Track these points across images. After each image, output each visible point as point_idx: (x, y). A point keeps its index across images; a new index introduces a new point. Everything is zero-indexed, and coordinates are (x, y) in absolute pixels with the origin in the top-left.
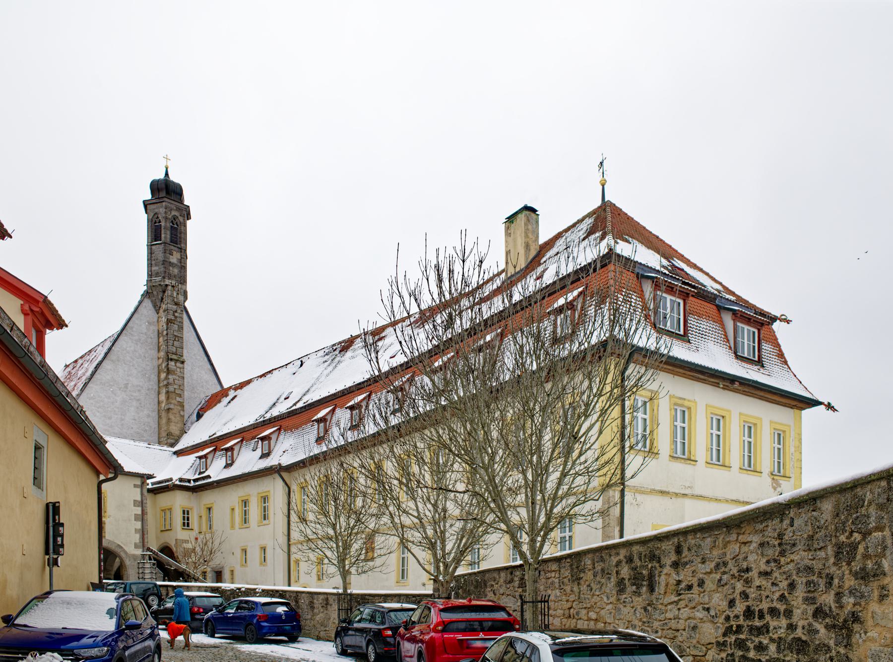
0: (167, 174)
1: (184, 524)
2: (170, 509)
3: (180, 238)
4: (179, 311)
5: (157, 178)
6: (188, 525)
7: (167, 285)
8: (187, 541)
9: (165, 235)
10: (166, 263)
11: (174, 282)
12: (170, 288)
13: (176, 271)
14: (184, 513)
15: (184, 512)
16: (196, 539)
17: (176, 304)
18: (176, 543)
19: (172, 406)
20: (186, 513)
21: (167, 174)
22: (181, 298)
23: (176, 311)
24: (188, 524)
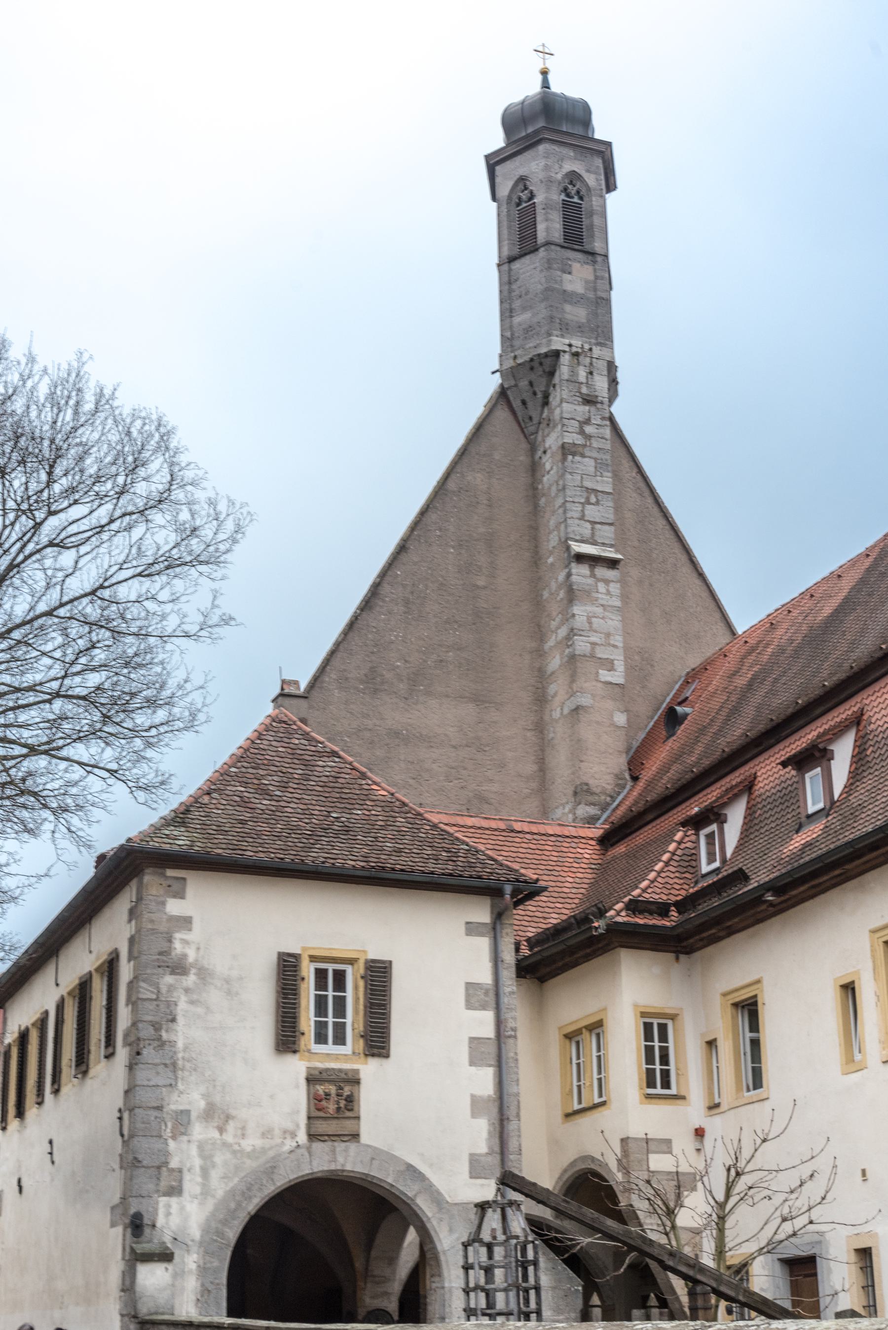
0: (546, 85)
1: (650, 1074)
2: (599, 1024)
3: (591, 227)
4: (596, 420)
5: (517, 98)
6: (666, 1084)
7: (557, 354)
8: (665, 1146)
9: (549, 226)
10: (554, 295)
11: (577, 343)
12: (565, 359)
13: (577, 313)
14: (648, 1036)
15: (648, 1027)
16: (699, 1133)
17: (590, 401)
18: (625, 1152)
19: (585, 700)
20: (656, 1031)
21: (546, 85)
22: (601, 384)
23: (588, 421)
24: (666, 1075)
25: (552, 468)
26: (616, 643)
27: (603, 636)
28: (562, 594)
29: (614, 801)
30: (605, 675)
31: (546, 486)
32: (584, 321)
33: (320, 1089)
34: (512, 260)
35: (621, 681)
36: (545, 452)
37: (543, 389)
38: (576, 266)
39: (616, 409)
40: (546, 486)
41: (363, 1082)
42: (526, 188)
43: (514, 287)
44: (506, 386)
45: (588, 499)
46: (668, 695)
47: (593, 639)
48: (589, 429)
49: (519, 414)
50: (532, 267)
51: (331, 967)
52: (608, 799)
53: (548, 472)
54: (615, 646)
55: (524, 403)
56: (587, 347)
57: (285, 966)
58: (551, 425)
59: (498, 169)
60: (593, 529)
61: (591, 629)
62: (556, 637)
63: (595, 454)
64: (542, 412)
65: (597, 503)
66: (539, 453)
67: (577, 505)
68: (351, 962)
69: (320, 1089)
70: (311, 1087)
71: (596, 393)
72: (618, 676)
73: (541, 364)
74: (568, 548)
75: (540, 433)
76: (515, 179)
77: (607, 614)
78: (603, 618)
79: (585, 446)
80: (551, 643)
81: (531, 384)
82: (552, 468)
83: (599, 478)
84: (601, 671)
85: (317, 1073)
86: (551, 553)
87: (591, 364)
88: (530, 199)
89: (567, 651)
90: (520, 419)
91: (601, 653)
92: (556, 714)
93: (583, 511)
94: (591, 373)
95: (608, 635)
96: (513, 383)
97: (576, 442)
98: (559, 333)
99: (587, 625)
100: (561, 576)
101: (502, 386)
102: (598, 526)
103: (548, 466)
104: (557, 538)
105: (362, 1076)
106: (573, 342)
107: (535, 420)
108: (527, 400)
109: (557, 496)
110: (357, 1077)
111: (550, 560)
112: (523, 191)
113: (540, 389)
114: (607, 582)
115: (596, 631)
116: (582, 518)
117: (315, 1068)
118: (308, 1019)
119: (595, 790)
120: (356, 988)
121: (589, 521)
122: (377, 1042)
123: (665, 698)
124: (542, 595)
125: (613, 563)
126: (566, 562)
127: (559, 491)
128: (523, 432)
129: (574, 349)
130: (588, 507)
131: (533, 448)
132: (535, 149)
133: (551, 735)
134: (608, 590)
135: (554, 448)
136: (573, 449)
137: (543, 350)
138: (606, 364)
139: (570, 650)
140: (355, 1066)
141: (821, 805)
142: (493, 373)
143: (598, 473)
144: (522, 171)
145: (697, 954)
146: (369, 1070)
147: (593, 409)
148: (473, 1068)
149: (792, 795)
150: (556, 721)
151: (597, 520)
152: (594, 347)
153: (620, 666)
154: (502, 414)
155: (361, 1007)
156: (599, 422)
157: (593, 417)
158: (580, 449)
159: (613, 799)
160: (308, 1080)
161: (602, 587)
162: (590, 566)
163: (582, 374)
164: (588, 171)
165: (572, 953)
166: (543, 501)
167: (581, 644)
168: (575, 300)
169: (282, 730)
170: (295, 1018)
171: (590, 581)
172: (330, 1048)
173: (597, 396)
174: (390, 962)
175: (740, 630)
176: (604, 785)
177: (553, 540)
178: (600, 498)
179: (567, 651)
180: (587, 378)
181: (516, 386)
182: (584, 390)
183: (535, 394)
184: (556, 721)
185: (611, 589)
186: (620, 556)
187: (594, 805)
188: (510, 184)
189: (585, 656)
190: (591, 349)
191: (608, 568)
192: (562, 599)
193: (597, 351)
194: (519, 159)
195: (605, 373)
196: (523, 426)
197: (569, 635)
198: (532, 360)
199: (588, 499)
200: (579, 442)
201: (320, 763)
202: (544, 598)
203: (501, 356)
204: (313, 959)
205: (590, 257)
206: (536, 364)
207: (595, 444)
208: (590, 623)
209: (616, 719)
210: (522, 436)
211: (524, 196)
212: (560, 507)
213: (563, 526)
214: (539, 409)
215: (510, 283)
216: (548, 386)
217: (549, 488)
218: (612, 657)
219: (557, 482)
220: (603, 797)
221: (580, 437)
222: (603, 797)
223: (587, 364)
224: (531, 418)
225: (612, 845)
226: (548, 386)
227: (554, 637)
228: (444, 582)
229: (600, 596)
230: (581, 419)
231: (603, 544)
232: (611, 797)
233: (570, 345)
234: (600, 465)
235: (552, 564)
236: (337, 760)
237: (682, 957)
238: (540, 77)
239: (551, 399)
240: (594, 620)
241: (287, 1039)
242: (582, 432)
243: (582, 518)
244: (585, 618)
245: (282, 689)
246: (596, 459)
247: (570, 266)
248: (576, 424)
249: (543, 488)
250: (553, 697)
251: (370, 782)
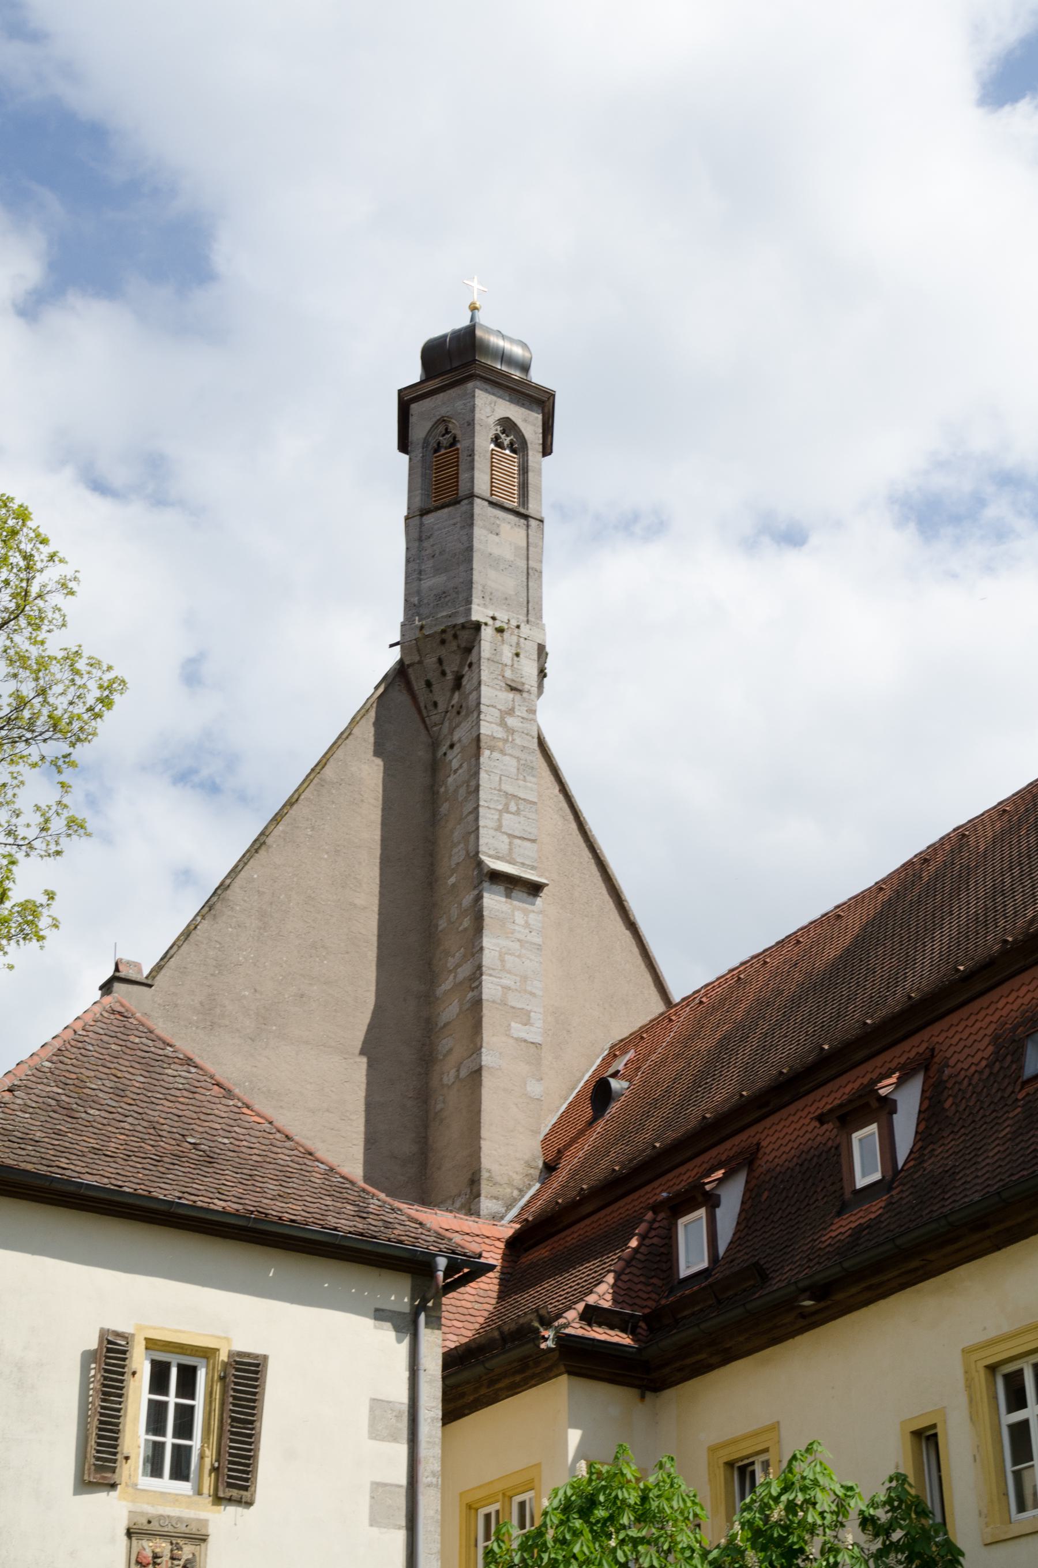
11: (503, 616)
12: (487, 634)
22: (529, 669)
23: (511, 712)
25: (461, 766)
26: (534, 991)
27: (518, 979)
28: (466, 923)
29: (523, 1196)
30: (518, 1030)
31: (451, 789)
32: (513, 593)
33: (148, 1547)
34: (424, 512)
35: (538, 1039)
36: (452, 746)
37: (456, 669)
39: (543, 705)
40: (451, 789)
41: (210, 1539)
42: (447, 432)
43: (425, 544)
44: (407, 663)
45: (507, 806)
46: (587, 1071)
47: (505, 982)
48: (510, 721)
49: (422, 700)
50: (452, 522)
51: (174, 1360)
52: (516, 1193)
53: (455, 772)
54: (532, 994)
55: (429, 684)
56: (514, 623)
57: (109, 1350)
58: (463, 713)
59: (414, 408)
60: (510, 843)
61: (503, 969)
62: (455, 977)
63: (517, 753)
64: (451, 697)
65: (518, 813)
66: (444, 748)
67: (493, 812)
68: (207, 1353)
69: (148, 1547)
70: (134, 1541)
71: (523, 680)
72: (533, 1034)
73: (455, 636)
74: (480, 863)
75: (446, 724)
76: (435, 420)
77: (524, 951)
78: (519, 956)
79: (506, 741)
80: (447, 985)
81: (440, 661)
82: (461, 766)
83: (521, 783)
84: (513, 1024)
85: (145, 1522)
86: (453, 871)
87: (518, 644)
88: (452, 445)
89: (470, 995)
90: (422, 705)
91: (514, 1001)
92: (449, 1078)
93: (499, 820)
94: (517, 655)
95: (525, 979)
96: (417, 659)
97: (495, 735)
98: (481, 601)
99: (499, 963)
100: (467, 900)
101: (401, 662)
102: (517, 841)
103: (455, 764)
104: (463, 853)
105: (212, 1530)
106: (497, 615)
107: (441, 707)
108: (433, 681)
109: (466, 799)
110: (203, 1532)
111: (452, 880)
112: (443, 435)
113: (450, 669)
115: (509, 972)
116: (499, 828)
117: (142, 1514)
118: (135, 1435)
119: (498, 1179)
120: (209, 1394)
121: (504, 833)
122: (236, 1479)
123: (583, 1076)
124: (436, 926)
125: (535, 889)
126: (476, 882)
127: (469, 793)
128: (424, 722)
129: (498, 624)
130: (506, 816)
131: (434, 745)
132: (462, 387)
133: (439, 1106)
134: (526, 922)
135: (465, 741)
136: (492, 743)
137: (461, 620)
138: (536, 647)
139: (475, 993)
140: (203, 1515)
141: (877, 1176)
142: (391, 646)
143: (521, 777)
144: (443, 411)
145: (669, 1394)
146: (221, 1521)
147: (518, 696)
148: (375, 1529)
149: (835, 1160)
150: (449, 1087)
151: (517, 833)
152: (522, 626)
153: (538, 1020)
154: (401, 697)
155: (215, 1424)
156: (525, 715)
157: (517, 707)
158: (500, 744)
159: (522, 1192)
160: (129, 1534)
162: (506, 888)
163: (507, 654)
164: (525, 420)
165: (492, 1383)
166: (445, 808)
167: (490, 985)
168: (502, 567)
169: (115, 1022)
170: (118, 1432)
172: (166, 1484)
173: (523, 684)
174: (265, 1358)
175: (676, 997)
176: (511, 1173)
177: (458, 854)
178: (521, 807)
179: (470, 995)
180: (513, 660)
181: (420, 662)
183: (444, 673)
184: (449, 1087)
185: (531, 921)
186: (543, 880)
187: (497, 1198)
188: (428, 425)
189: (494, 1002)
190: (518, 627)
191: (529, 894)
192: (466, 929)
193: (525, 630)
194: (441, 396)
195: (535, 657)
196: (425, 714)
197: (474, 973)
198: (443, 631)
199: (507, 806)
200: (499, 736)
201: (169, 1072)
202: (440, 928)
203: (403, 625)
204: (151, 1344)
205: (523, 521)
206: (448, 636)
207: (518, 741)
208: (503, 961)
209: (529, 1089)
210: (422, 726)
211: (445, 441)
212: (471, 813)
213: (473, 836)
214: (448, 694)
215: (420, 540)
216: (461, 666)
217: (456, 791)
218: (529, 1008)
219: (468, 782)
220: (508, 1190)
221: (500, 729)
222: (508, 1190)
223: (514, 644)
224: (435, 704)
225: (526, 1250)
226: (461, 666)
227: (451, 977)
228: (313, 895)
229: (517, 928)
230: (503, 708)
231: (523, 864)
232: (520, 1191)
233: (494, 618)
235: (453, 885)
236: (193, 1070)
237: (649, 1395)
238: (470, 314)
239: (464, 681)
240: (507, 957)
241: (99, 1464)
242: (503, 723)
244: (497, 954)
245: (117, 969)
246: (518, 759)
247: (498, 526)
248: (497, 713)
249: (446, 791)
250: (445, 1056)
251: (240, 1104)
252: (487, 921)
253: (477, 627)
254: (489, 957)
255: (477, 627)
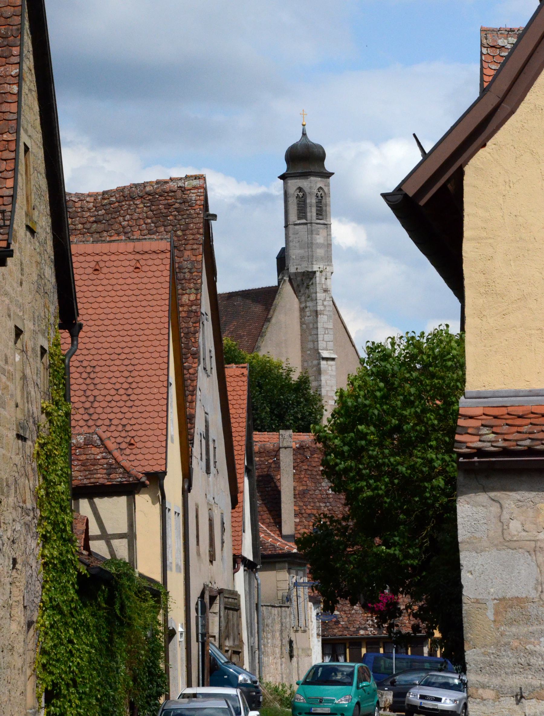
4: (328, 299)
12: (318, 274)
21: (304, 134)
23: (325, 300)
38: (321, 231)
48: (325, 303)
81: (302, 280)
114: (331, 366)
125: (333, 359)
161: (330, 368)
171: (326, 366)
182: (324, 287)
234: (329, 317)
242: (323, 305)
243: (323, 340)
252: (322, 371)
253: (314, 273)
254: (323, 382)
255: (314, 273)
